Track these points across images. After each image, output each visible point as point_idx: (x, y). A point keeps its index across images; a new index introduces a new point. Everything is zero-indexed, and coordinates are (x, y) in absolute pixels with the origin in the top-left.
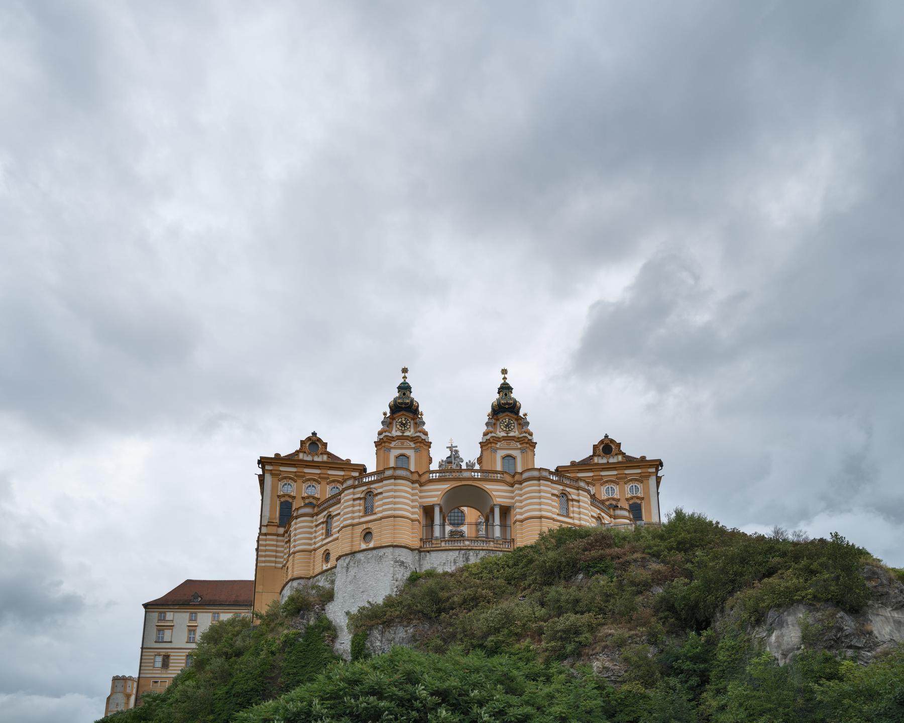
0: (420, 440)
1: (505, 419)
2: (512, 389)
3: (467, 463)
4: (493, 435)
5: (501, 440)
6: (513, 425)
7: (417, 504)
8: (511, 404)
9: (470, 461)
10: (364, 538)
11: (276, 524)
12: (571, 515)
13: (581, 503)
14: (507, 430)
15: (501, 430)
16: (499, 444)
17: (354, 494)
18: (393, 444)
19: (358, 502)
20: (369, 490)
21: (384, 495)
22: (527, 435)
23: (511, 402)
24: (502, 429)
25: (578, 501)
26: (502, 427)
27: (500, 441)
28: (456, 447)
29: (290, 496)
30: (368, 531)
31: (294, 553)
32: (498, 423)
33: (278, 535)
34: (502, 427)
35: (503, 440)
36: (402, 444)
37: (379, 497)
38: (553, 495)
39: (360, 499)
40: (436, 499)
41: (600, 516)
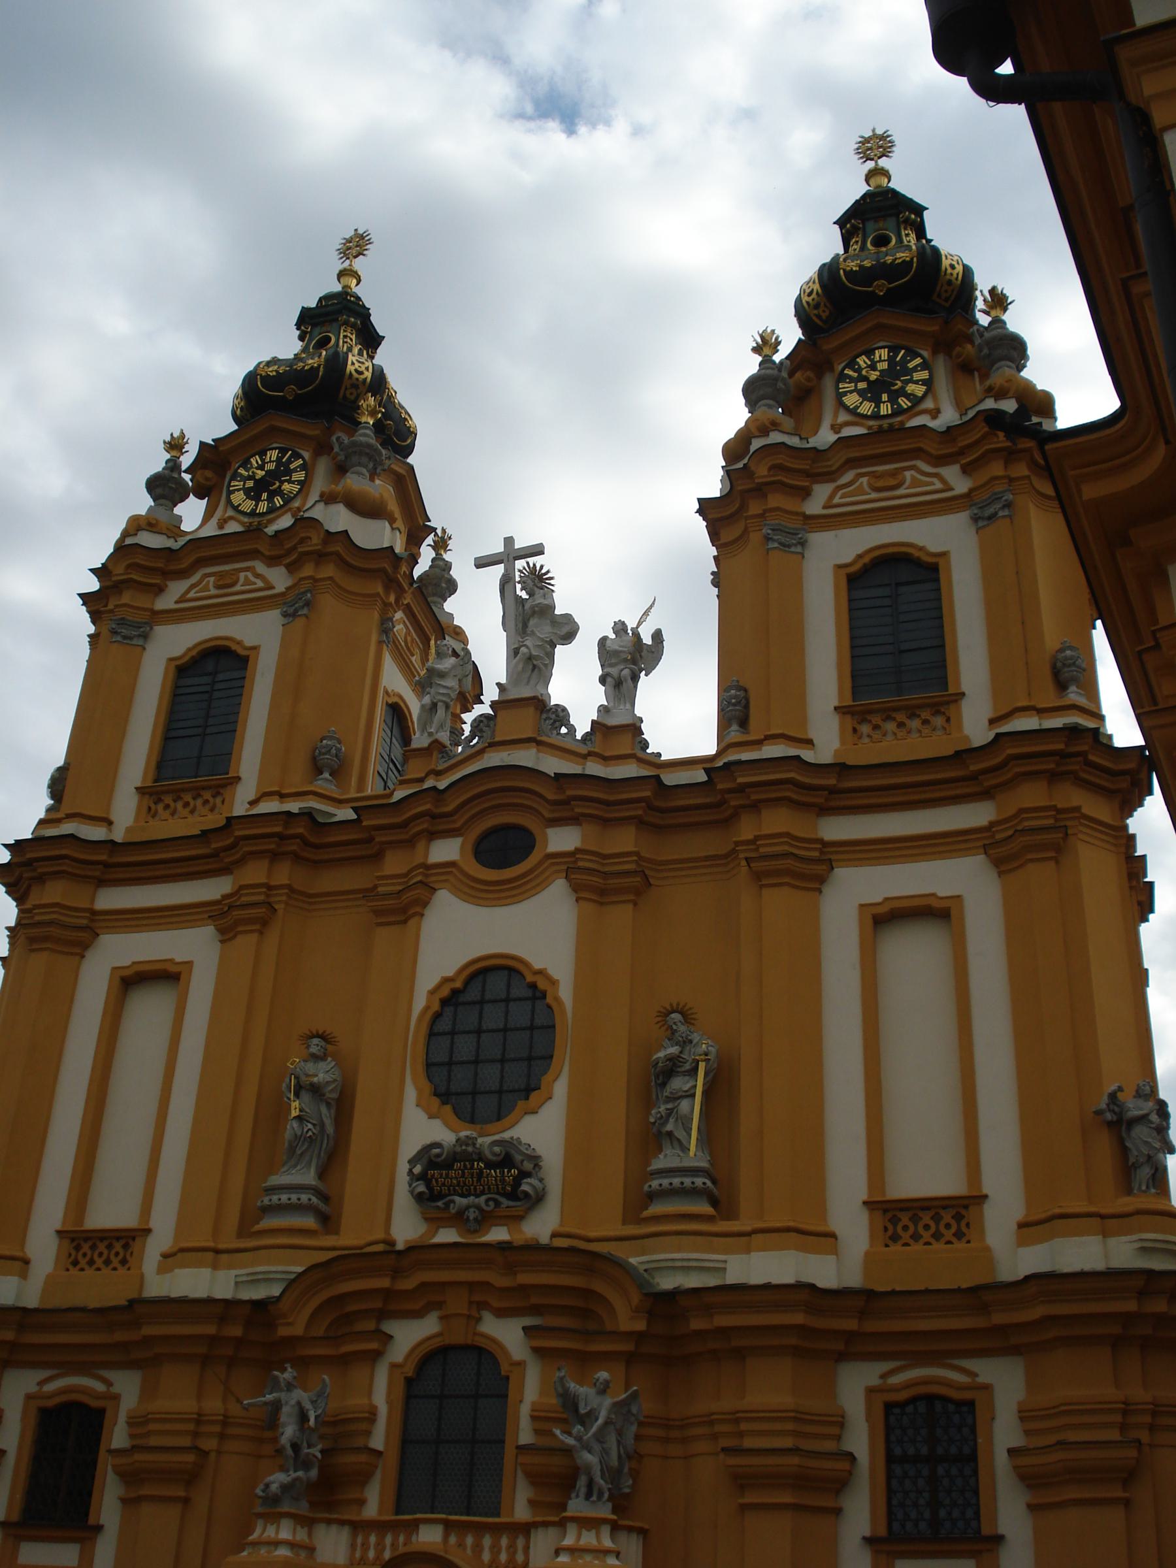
0: (316, 541)
1: (869, 353)
2: (919, 210)
3: (603, 642)
4: (775, 437)
5: (836, 462)
6: (924, 375)
9: (620, 627)
15: (843, 417)
18: (172, 595)
26: (851, 400)
27: (828, 476)
28: (538, 550)
32: (828, 381)
34: (851, 400)
35: (851, 463)
36: (225, 582)
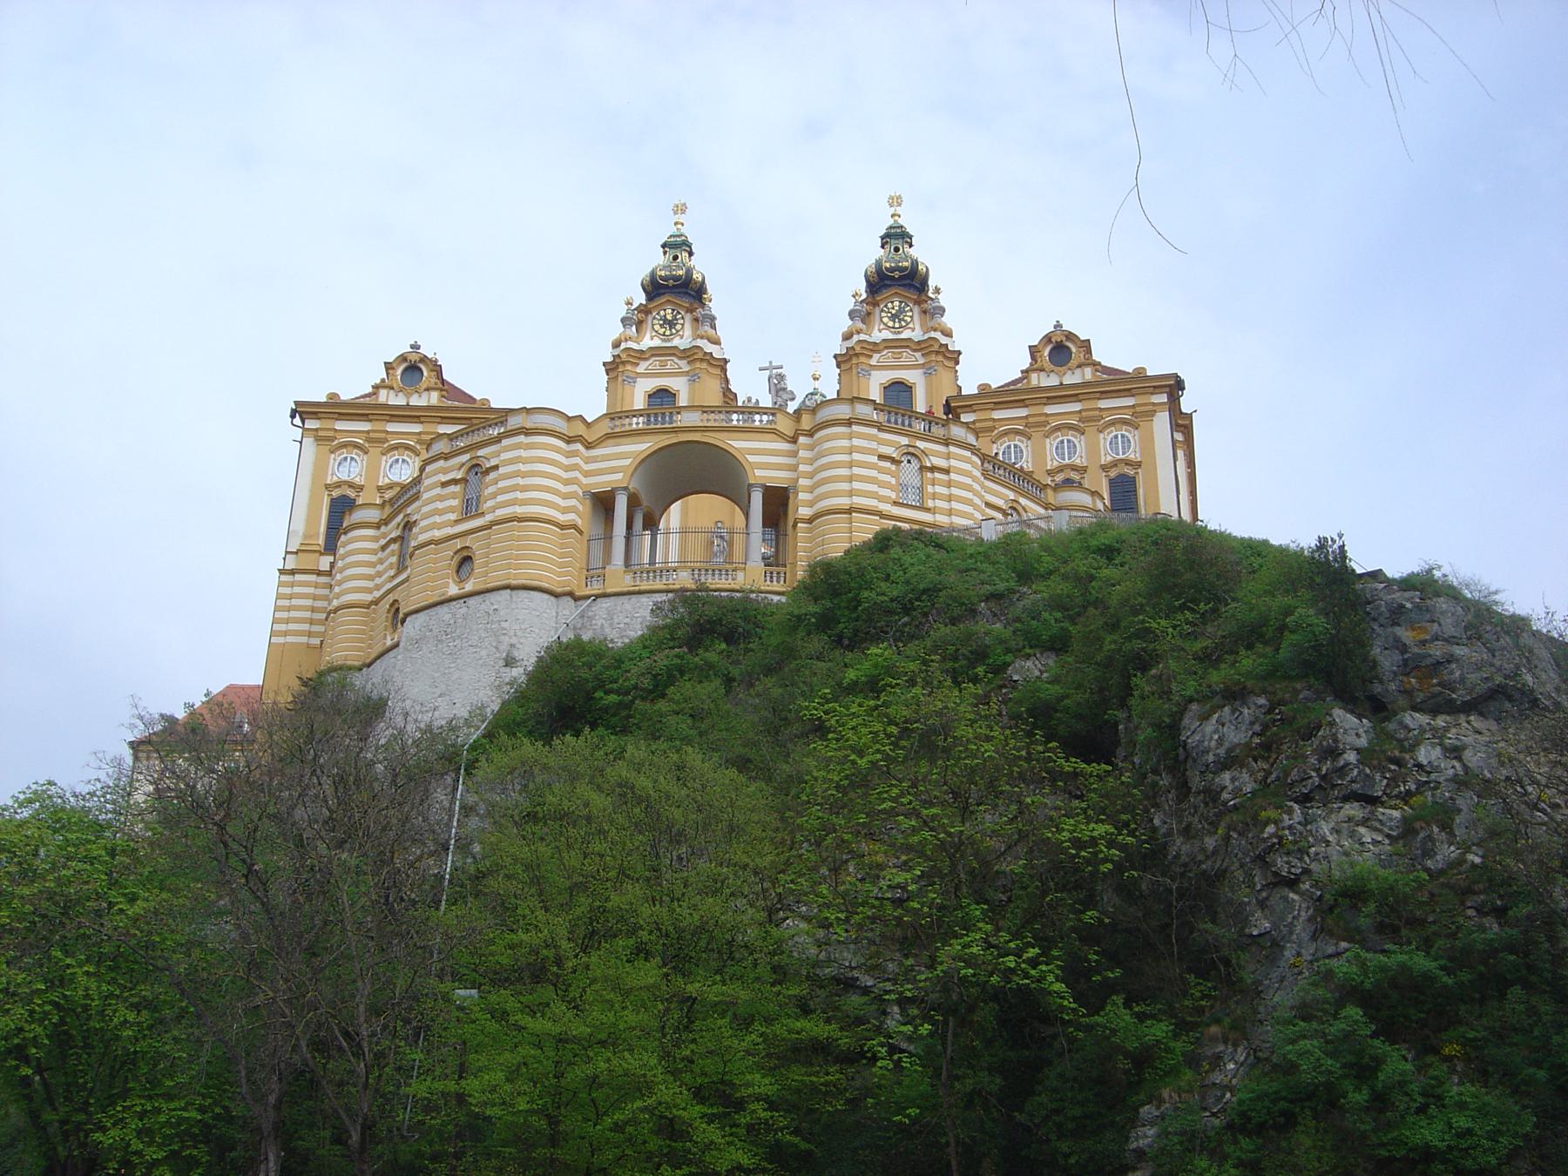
1: (892, 302)
5: (881, 348)
7: (574, 488)
8: (902, 269)
10: (458, 572)
11: (317, 548)
12: (930, 504)
13: (953, 476)
14: (897, 325)
15: (882, 326)
16: (876, 356)
17: (445, 471)
19: (453, 488)
20: (474, 462)
21: (502, 470)
22: (937, 335)
23: (906, 264)
24: (886, 325)
25: (947, 471)
26: (885, 320)
27: (879, 352)
29: (351, 485)
30: (465, 554)
31: (336, 610)
32: (877, 310)
33: (319, 573)
34: (885, 320)
35: (887, 348)
37: (493, 475)
38: (881, 457)
39: (454, 482)
40: (620, 476)
41: (1015, 505)
